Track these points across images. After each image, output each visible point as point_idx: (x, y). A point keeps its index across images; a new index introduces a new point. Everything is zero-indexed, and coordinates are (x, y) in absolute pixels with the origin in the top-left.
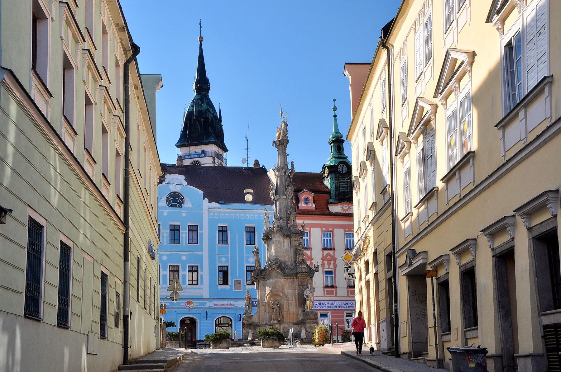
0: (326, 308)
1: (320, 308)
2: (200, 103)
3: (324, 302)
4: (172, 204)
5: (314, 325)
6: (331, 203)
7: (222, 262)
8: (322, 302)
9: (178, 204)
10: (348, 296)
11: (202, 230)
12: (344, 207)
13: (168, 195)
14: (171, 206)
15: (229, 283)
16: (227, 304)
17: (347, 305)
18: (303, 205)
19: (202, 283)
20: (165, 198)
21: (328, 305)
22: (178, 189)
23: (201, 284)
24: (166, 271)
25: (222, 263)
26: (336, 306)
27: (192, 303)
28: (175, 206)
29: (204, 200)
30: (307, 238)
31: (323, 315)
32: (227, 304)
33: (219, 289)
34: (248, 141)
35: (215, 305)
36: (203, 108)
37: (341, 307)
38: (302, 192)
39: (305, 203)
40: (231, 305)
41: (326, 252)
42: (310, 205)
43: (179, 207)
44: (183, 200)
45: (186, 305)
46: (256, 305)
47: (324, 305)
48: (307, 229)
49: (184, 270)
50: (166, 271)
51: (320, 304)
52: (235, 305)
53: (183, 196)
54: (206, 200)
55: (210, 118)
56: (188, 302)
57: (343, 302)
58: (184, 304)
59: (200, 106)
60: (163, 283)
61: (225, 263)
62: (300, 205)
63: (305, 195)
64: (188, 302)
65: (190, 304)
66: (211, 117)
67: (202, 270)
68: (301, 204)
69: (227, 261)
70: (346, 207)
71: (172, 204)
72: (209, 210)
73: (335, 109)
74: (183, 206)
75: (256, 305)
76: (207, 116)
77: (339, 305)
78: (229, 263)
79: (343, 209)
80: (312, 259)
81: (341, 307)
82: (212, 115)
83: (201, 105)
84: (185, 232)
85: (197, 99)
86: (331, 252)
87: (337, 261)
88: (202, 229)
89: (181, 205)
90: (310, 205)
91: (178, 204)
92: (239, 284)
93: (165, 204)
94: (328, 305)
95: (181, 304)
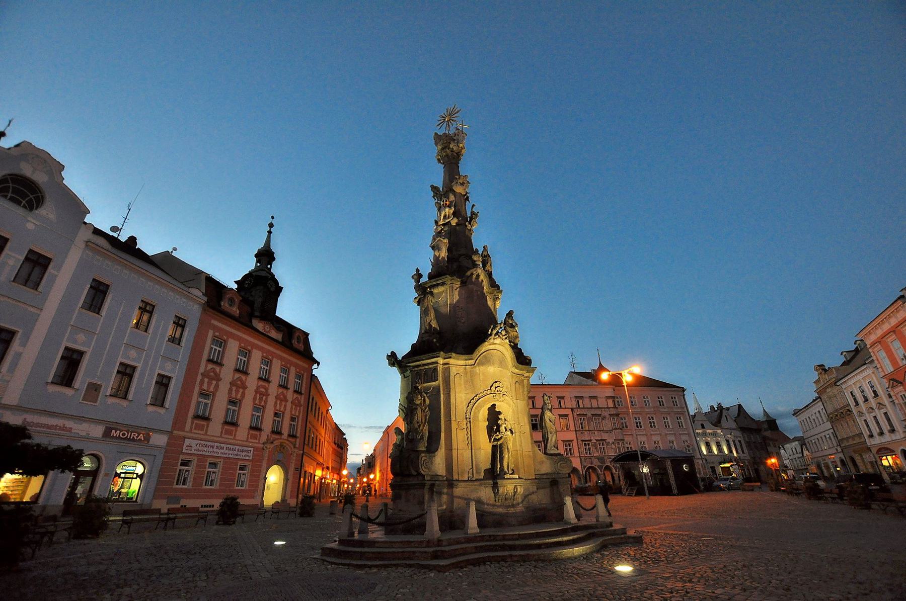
0: (219, 455)
1: (211, 454)
3: (219, 445)
6: (256, 317)
8: (216, 444)
10: (247, 441)
11: (59, 270)
12: (266, 329)
16: (57, 426)
17: (244, 453)
18: (227, 305)
21: (222, 451)
26: (231, 452)
30: (220, 349)
31: (214, 465)
34: (130, 210)
37: (237, 455)
40: (64, 428)
41: (237, 375)
42: (234, 309)
43: (24, 207)
46: (114, 436)
47: (218, 450)
51: (213, 447)
52: (73, 431)
57: (241, 448)
67: (24, 344)
70: (268, 328)
72: (89, 243)
73: (271, 225)
75: (114, 436)
77: (235, 453)
78: (89, 347)
79: (264, 327)
80: (221, 379)
81: (237, 455)
86: (243, 377)
87: (246, 391)
88: (59, 268)
90: (234, 309)
92: (96, 390)
94: (222, 451)
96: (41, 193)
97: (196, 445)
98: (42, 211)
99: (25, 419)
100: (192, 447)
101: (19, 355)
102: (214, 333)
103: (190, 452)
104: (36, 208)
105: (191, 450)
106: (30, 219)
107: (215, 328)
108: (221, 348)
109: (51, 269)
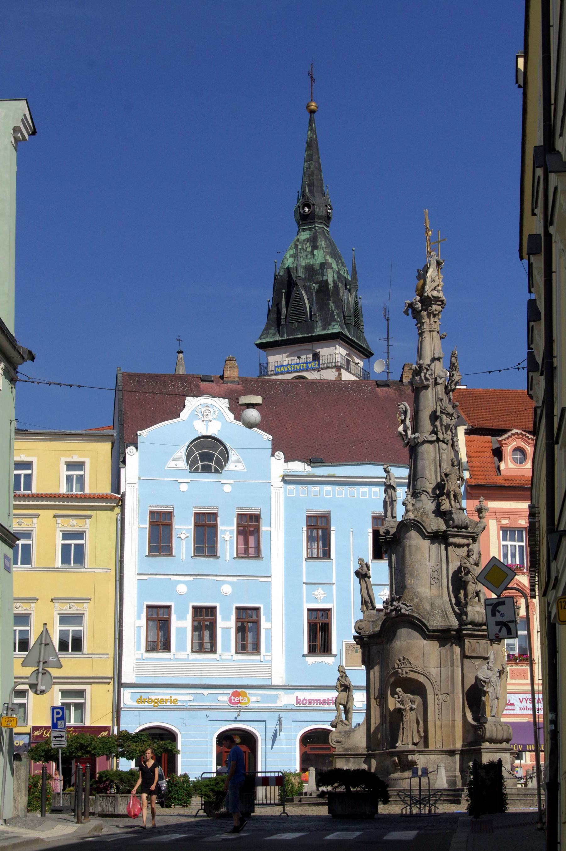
2: (309, 249)
4: (200, 464)
7: (316, 600)
9: (213, 465)
13: (191, 443)
14: (196, 471)
15: (335, 651)
16: (328, 699)
18: (511, 465)
19: (269, 649)
20: (183, 452)
22: (213, 429)
23: (267, 651)
24: (186, 619)
25: (317, 602)
27: (245, 695)
28: (206, 469)
29: (273, 455)
32: (328, 699)
33: (310, 663)
34: (388, 320)
35: (298, 701)
36: (316, 260)
38: (509, 434)
39: (515, 460)
43: (216, 471)
44: (225, 453)
45: (230, 699)
48: (520, 522)
50: (186, 619)
53: (225, 447)
54: (280, 454)
55: (331, 282)
56: (236, 694)
58: (226, 698)
59: (309, 256)
60: (178, 649)
61: (324, 601)
62: (502, 466)
63: (515, 443)
64: (236, 694)
65: (241, 698)
66: (334, 280)
68: (506, 464)
69: (328, 598)
74: (226, 469)
76: (325, 278)
82: (336, 276)
83: (312, 253)
84: (230, 530)
85: (304, 240)
91: (213, 465)
93: (183, 464)
95: (220, 698)
96: (222, 443)
97: (521, 702)
98: (230, 466)
99: (297, 697)
100: (513, 704)
101: (269, 632)
102: (499, 522)
103: (512, 712)
104: (225, 466)
105: (514, 710)
106: (224, 481)
107: (497, 514)
108: (522, 541)
109: (264, 528)
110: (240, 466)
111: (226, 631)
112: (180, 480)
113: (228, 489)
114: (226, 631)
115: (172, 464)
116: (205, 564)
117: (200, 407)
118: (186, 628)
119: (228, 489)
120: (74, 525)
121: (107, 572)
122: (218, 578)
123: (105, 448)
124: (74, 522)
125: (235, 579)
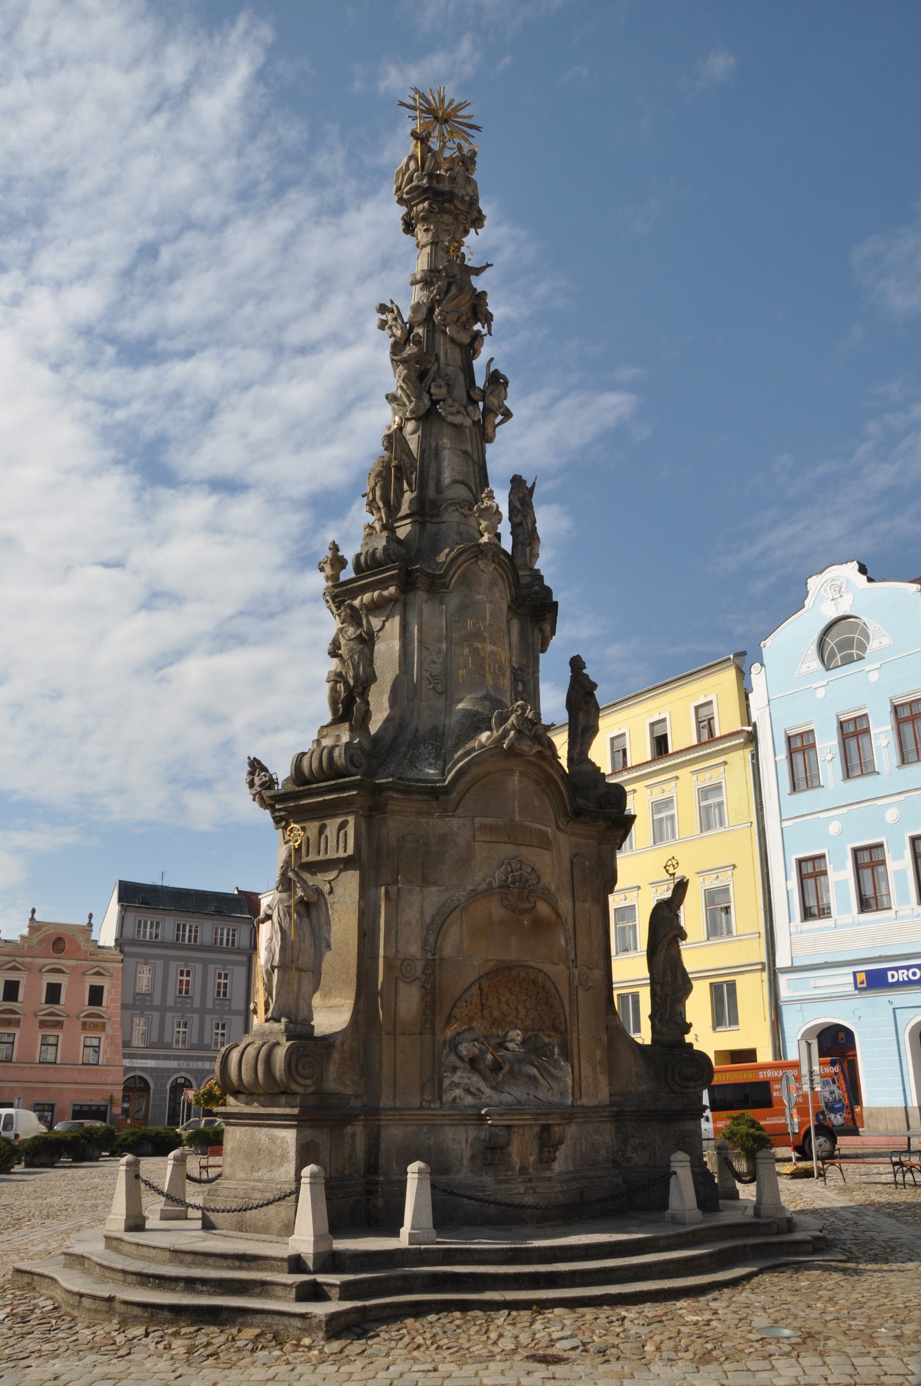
5: (273, 1140)
43: (861, 658)
49: (899, 856)
71: (838, 656)
74: (868, 651)
89: (863, 648)
98: (873, 645)
110: (886, 641)
111: (901, 873)
112: (815, 686)
113: (874, 677)
114: (901, 873)
115: (804, 669)
116: (861, 786)
117: (825, 585)
118: (847, 880)
119: (874, 677)
120: (707, 779)
121: (747, 826)
122: (879, 802)
123: (729, 676)
124: (707, 775)
125: (902, 797)
